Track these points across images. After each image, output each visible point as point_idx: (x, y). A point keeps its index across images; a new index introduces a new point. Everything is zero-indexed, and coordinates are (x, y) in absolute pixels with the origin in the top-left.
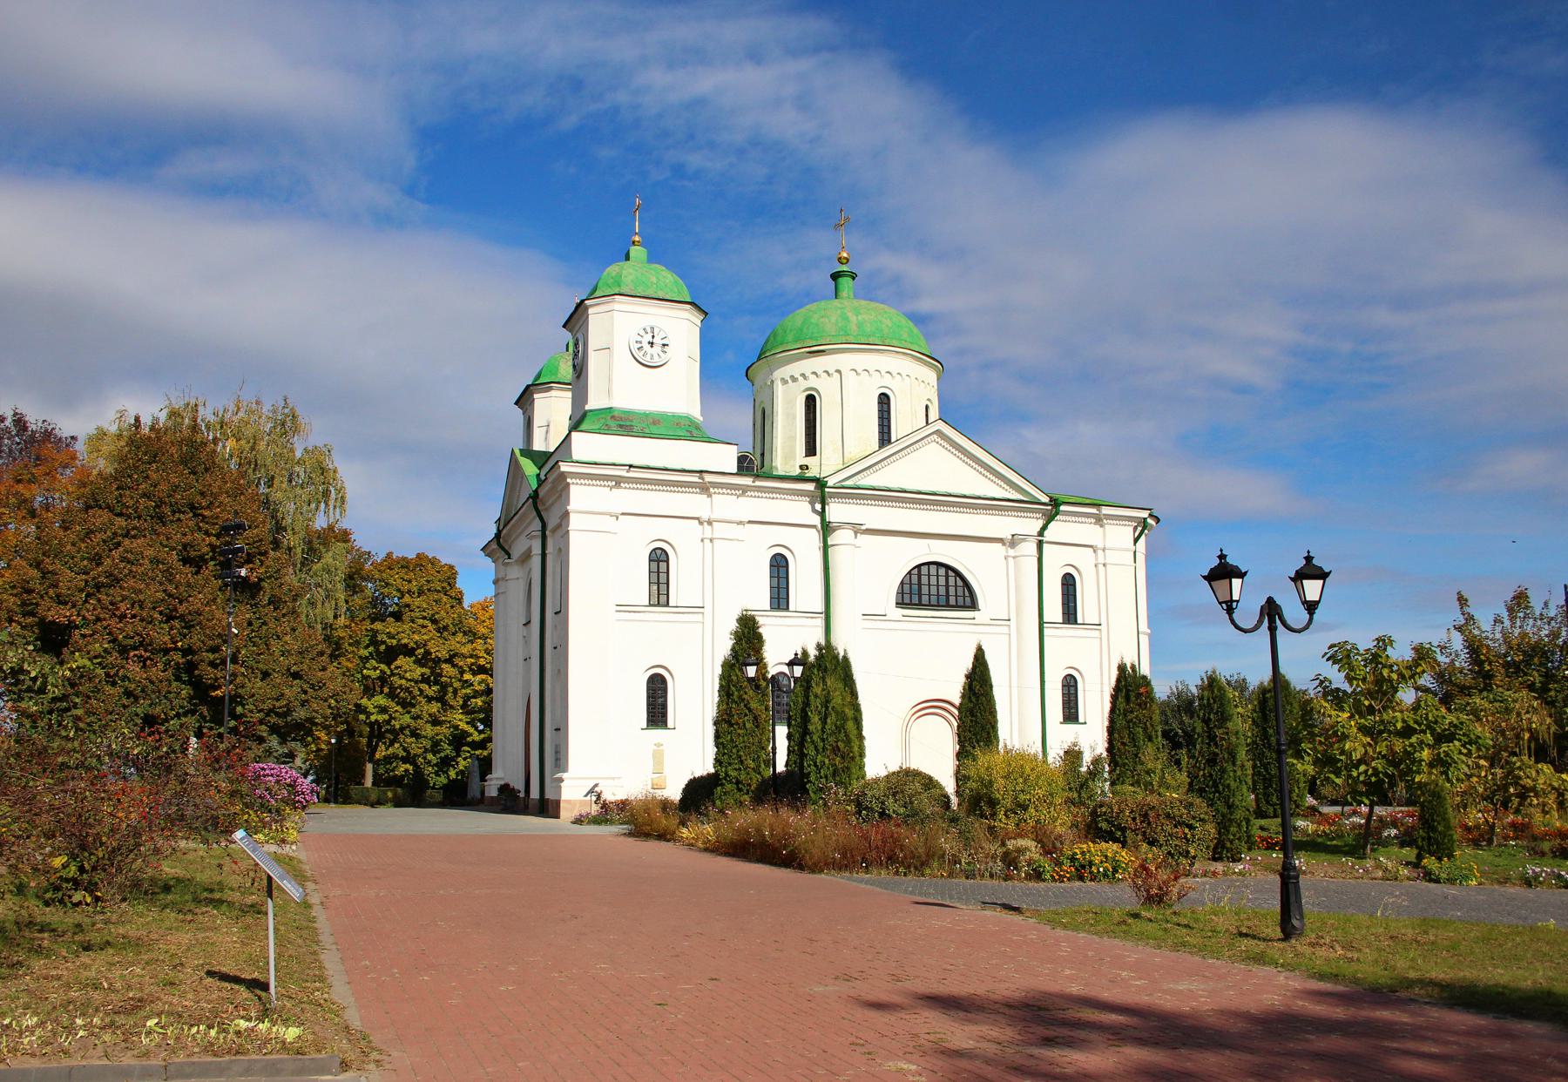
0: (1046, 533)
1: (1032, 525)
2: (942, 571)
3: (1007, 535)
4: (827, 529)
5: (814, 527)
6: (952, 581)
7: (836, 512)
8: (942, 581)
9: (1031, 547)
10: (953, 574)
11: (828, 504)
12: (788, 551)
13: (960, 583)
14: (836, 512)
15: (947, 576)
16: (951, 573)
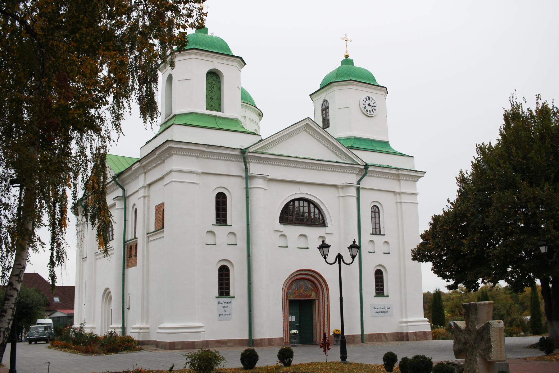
0: (361, 182)
1: (353, 179)
2: (306, 204)
3: (340, 183)
4: (248, 178)
5: (241, 176)
6: (312, 210)
7: (254, 168)
8: (306, 210)
9: (353, 192)
10: (313, 206)
11: (249, 162)
12: (228, 192)
13: (317, 211)
14: (254, 168)
15: (309, 207)
16: (311, 205)
